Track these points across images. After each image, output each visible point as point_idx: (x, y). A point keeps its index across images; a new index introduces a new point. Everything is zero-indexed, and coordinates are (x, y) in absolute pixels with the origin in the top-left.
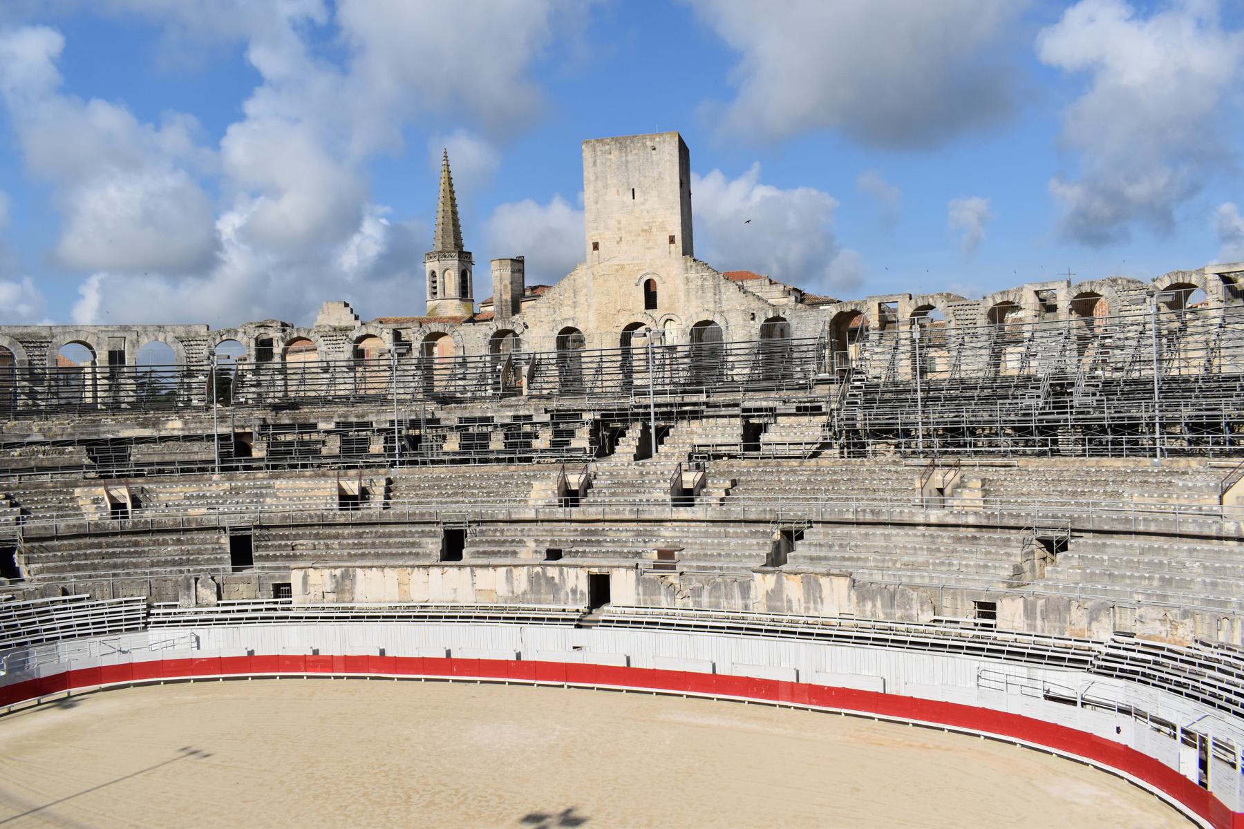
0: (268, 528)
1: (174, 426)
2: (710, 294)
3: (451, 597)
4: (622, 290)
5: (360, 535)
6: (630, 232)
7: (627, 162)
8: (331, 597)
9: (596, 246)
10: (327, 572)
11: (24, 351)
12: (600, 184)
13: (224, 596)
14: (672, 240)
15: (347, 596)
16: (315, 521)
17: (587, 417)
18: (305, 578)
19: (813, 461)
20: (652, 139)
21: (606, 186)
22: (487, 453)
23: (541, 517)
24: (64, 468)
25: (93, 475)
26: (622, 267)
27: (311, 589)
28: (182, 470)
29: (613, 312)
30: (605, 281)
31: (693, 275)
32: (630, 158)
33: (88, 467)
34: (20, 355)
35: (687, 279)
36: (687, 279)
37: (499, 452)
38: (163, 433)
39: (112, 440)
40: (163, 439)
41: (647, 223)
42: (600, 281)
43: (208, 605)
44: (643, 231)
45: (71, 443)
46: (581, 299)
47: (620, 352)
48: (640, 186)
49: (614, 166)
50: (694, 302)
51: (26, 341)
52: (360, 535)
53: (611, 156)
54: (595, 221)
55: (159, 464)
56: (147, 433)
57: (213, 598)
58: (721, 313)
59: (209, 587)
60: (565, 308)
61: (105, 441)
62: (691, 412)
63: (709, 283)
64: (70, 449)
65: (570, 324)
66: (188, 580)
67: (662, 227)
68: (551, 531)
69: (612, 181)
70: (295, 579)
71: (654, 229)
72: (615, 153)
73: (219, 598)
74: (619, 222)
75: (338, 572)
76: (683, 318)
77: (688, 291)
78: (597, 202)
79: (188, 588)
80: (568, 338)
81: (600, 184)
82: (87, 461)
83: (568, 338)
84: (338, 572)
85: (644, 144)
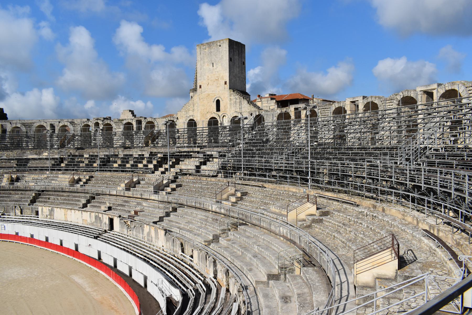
0: (48, 191)
1: (45, 154)
2: (238, 105)
3: (76, 221)
5: (68, 196)
6: (212, 80)
7: (211, 52)
8: (49, 217)
9: (200, 87)
10: (47, 208)
11: (25, 128)
12: (202, 62)
13: (23, 213)
14: (226, 83)
15: (52, 217)
16: (60, 190)
17: (159, 155)
18: (42, 209)
19: (213, 179)
20: (220, 42)
21: (204, 63)
23: (118, 194)
24: (8, 167)
25: (15, 170)
26: (209, 95)
27: (44, 214)
28: (40, 170)
29: (206, 113)
30: (203, 100)
31: (232, 97)
32: (212, 51)
33: (15, 167)
34: (24, 129)
37: (129, 168)
38: (41, 157)
39: (25, 159)
40: (40, 159)
41: (217, 77)
42: (202, 100)
43: (18, 216)
44: (216, 80)
45: (13, 160)
46: (195, 108)
47: (207, 128)
48: (215, 62)
49: (207, 54)
50: (233, 109)
51: (24, 124)
52: (68, 196)
53: (206, 50)
54: (200, 77)
55: (34, 167)
56: (35, 157)
57: (19, 214)
59: (18, 210)
60: (190, 112)
61: (23, 159)
62: (186, 155)
63: (238, 101)
64: (12, 161)
65: (192, 118)
66: (13, 207)
67: (222, 78)
68: (116, 200)
69: (206, 60)
70: (40, 209)
71: (220, 79)
72: (207, 49)
73: (21, 213)
74: (208, 77)
75: (50, 208)
76: (229, 115)
77: (231, 104)
78: (201, 69)
79: (13, 209)
80: (192, 124)
81: (202, 62)
82: (15, 166)
83: (192, 124)
84: (50, 208)
85: (217, 44)
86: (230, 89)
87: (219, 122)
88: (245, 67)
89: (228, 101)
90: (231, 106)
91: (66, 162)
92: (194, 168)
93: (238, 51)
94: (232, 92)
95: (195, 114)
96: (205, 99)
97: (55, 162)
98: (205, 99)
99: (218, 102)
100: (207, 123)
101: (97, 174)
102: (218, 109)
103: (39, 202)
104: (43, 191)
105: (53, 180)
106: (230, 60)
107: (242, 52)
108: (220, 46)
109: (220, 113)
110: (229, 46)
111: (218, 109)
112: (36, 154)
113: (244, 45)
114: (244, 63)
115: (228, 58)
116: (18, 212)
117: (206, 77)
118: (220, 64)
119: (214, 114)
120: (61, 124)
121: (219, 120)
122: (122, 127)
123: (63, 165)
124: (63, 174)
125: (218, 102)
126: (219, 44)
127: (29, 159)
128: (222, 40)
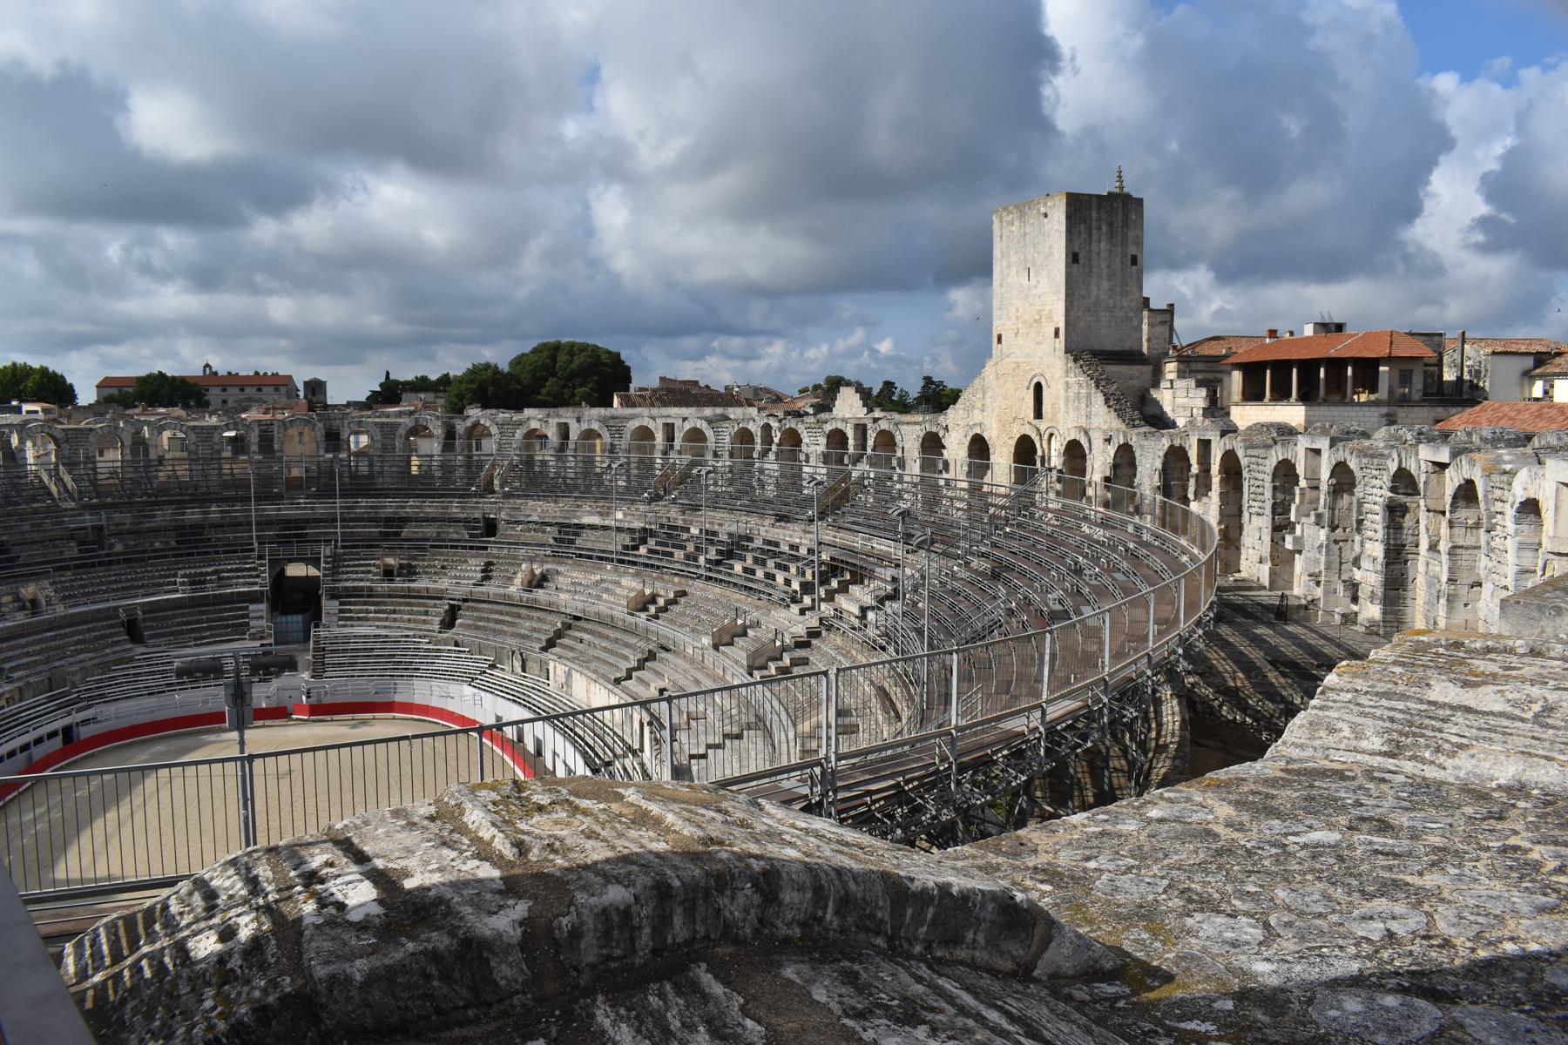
21: (1009, 267)
22: (751, 580)
31: (1072, 380)
38: (607, 523)
40: (605, 528)
41: (1038, 312)
45: (551, 525)
46: (988, 401)
50: (1072, 414)
57: (519, 670)
58: (1086, 433)
67: (1050, 317)
69: (1014, 259)
72: (1017, 223)
80: (979, 447)
82: (552, 541)
87: (1039, 453)
89: (1061, 386)
91: (652, 543)
92: (857, 612)
93: (1110, 225)
94: (1071, 364)
95: (986, 422)
97: (633, 540)
99: (1038, 388)
101: (697, 588)
102: (1038, 414)
103: (564, 647)
104: (577, 618)
105: (607, 590)
106: (1073, 258)
107: (1126, 224)
109: (1042, 425)
110: (1068, 217)
111: (1038, 414)
112: (601, 514)
113: (1140, 202)
114: (1134, 260)
116: (517, 665)
117: (1012, 310)
118: (1045, 273)
120: (687, 426)
122: (823, 441)
123: (643, 550)
124: (636, 575)
125: (1038, 388)
126: (1043, 210)
127: (582, 527)
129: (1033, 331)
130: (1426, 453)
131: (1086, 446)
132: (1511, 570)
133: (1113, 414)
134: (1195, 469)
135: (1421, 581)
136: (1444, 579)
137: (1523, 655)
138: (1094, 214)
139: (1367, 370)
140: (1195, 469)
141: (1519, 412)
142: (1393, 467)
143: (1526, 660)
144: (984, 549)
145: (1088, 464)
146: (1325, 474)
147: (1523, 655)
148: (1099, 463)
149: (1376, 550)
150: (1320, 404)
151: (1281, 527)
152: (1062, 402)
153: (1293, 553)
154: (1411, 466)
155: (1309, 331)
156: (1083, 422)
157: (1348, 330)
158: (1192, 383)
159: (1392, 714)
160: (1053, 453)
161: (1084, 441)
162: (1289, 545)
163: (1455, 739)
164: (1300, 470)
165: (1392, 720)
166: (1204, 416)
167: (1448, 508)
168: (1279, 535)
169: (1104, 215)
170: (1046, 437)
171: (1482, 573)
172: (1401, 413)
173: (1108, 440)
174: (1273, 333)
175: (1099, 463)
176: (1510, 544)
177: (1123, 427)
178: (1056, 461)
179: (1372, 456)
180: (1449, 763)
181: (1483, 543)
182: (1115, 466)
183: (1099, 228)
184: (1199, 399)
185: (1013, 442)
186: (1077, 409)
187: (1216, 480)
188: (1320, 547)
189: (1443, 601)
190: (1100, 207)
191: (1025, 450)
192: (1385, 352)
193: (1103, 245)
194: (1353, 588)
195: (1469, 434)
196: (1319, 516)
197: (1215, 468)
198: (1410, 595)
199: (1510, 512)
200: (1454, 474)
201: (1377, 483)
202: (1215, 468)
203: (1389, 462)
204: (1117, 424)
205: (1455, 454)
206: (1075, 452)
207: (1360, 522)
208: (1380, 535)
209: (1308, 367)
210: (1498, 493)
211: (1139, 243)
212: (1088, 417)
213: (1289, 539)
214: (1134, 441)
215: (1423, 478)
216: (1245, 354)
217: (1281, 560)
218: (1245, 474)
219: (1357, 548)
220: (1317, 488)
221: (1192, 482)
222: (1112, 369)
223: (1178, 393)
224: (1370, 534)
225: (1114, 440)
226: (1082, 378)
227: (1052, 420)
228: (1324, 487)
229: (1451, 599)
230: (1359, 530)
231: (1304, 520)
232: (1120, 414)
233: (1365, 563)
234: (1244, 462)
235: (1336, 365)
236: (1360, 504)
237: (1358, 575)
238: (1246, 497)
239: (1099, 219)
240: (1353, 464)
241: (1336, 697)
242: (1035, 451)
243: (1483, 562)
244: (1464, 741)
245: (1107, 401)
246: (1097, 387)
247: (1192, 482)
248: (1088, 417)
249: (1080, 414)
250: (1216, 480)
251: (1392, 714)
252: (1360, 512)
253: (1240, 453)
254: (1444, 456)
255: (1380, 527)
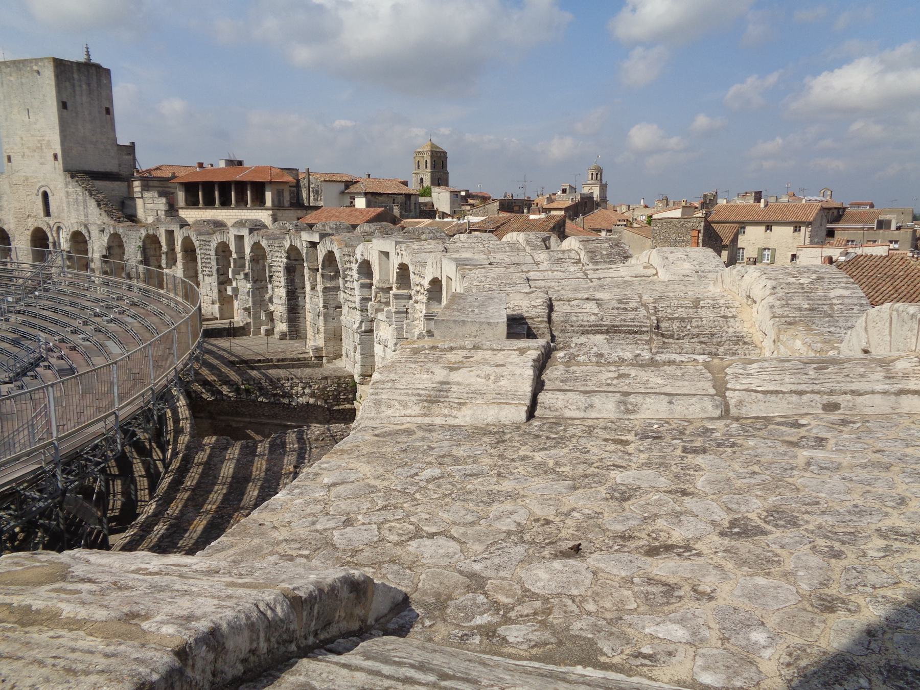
2: (82, 208)
4: (29, 198)
7: (22, 84)
14: (55, 157)
20: (36, 64)
31: (71, 190)
32: (24, 81)
35: (67, 192)
36: (67, 192)
41: (39, 141)
42: (14, 188)
44: (37, 147)
50: (73, 214)
58: (86, 226)
63: (80, 198)
74: (22, 138)
78: (6, 120)
85: (31, 67)
86: (65, 171)
87: (51, 239)
88: (112, 120)
89: (63, 194)
90: (69, 208)
93: (89, 85)
94: (69, 179)
96: (21, 187)
98: (21, 187)
99: (45, 196)
100: (29, 238)
102: (47, 213)
106: (63, 105)
108: (38, 72)
111: (47, 213)
114: (108, 111)
115: (55, 104)
117: (18, 139)
119: (41, 222)
121: (49, 234)
125: (45, 196)
126: (35, 68)
128: (42, 59)
129: (36, 154)
130: (306, 236)
131: (86, 235)
132: (357, 299)
133: (104, 214)
134: (164, 248)
135: (308, 306)
136: (321, 305)
137: (470, 349)
138: (76, 76)
139: (259, 189)
140: (164, 248)
141: (340, 213)
142: (287, 245)
143: (473, 352)
144: (19, 309)
145: (89, 246)
146: (247, 250)
147: (470, 349)
148: (97, 246)
149: (282, 292)
150: (233, 209)
151: (224, 281)
152: (64, 205)
153: (231, 297)
154: (298, 244)
155: (222, 164)
156: (82, 218)
157: (246, 165)
158: (156, 195)
159: (418, 391)
160: (62, 240)
161: (84, 232)
162: (229, 292)
163: (457, 401)
164: (232, 248)
165: (419, 395)
166: (166, 216)
167: (320, 267)
168: (223, 287)
169: (83, 78)
170: (55, 229)
171: (342, 301)
172: (279, 214)
173: (103, 231)
174: (201, 165)
175: (97, 246)
176: (356, 285)
177: (112, 222)
178: (65, 245)
179: (274, 239)
180: (459, 414)
181: (341, 285)
182: (109, 248)
183: (81, 86)
184: (161, 204)
185: (29, 233)
186: (77, 210)
187: (179, 256)
188: (248, 292)
189: (321, 318)
190: (79, 70)
191: (39, 239)
192: (268, 179)
193: (85, 99)
194: (270, 315)
195: (324, 226)
196: (246, 275)
197: (178, 248)
198: (301, 315)
199: (355, 267)
200: (322, 248)
201: (277, 254)
202: (178, 248)
203: (285, 242)
204: (106, 219)
205: (322, 236)
206: (79, 239)
207: (271, 277)
208: (283, 284)
209: (225, 187)
210: (347, 258)
211: (110, 98)
212: (86, 215)
213: (229, 289)
214: (120, 231)
215: (305, 251)
216: (183, 176)
217: (225, 301)
218: (198, 251)
219: (270, 291)
220: (243, 258)
221: (164, 257)
222: (98, 184)
223: (147, 201)
224: (276, 283)
225: (106, 231)
226: (79, 189)
227: (58, 217)
228: (247, 258)
229: (325, 317)
230: (270, 282)
231: (237, 277)
232: (109, 214)
233: (275, 301)
234: (197, 244)
235: (241, 186)
236: (270, 267)
237: (272, 308)
238: (199, 265)
239: (80, 80)
240: (264, 243)
241: (382, 386)
242: (48, 239)
243: (342, 295)
244: (462, 401)
245: (99, 205)
246: (91, 195)
247: (164, 257)
248: (86, 215)
249: (77, 211)
250: (179, 256)
251: (418, 391)
252: (270, 272)
253: (194, 239)
254: (316, 238)
255: (282, 280)
